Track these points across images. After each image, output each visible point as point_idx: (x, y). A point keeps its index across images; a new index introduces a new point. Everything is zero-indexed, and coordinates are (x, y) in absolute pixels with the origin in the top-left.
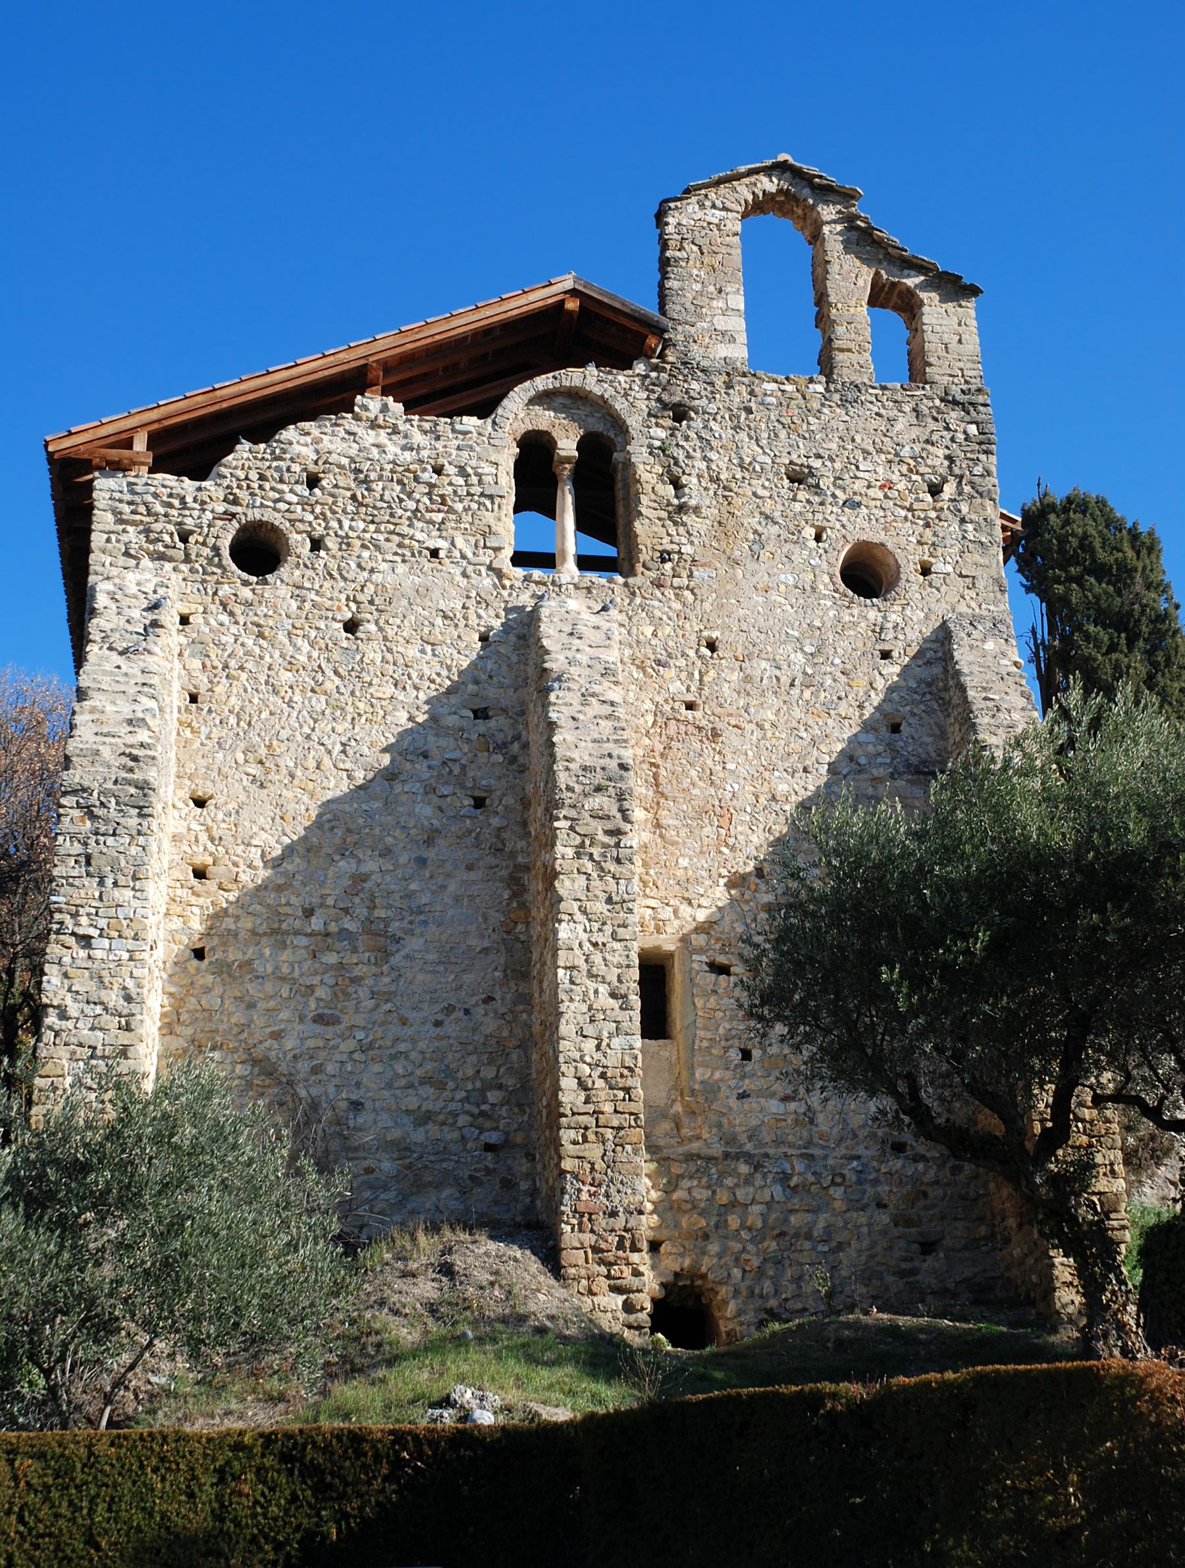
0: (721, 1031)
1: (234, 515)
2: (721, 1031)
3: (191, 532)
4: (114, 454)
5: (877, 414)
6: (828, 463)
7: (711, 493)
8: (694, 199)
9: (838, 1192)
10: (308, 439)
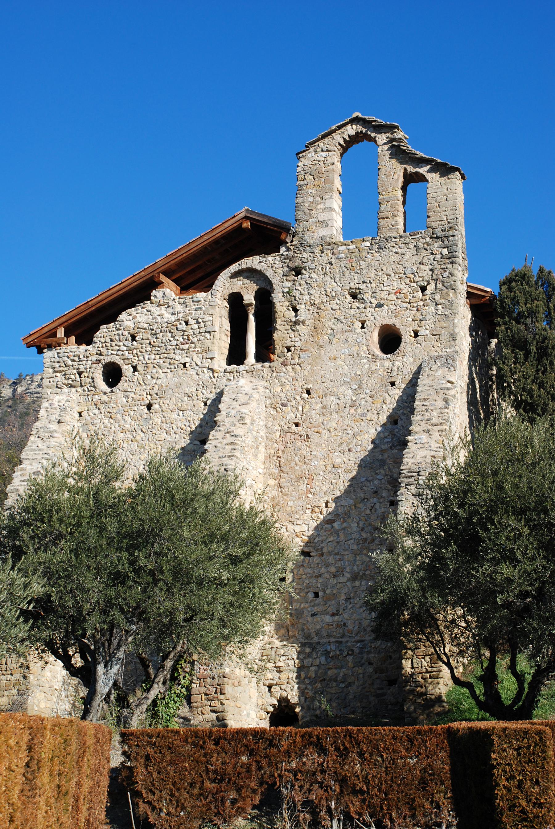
0: (305, 585)
1: (100, 361)
2: (305, 585)
3: (83, 372)
4: (49, 340)
5: (396, 253)
6: (369, 285)
7: (311, 311)
8: (312, 149)
9: (350, 658)
10: (131, 317)
